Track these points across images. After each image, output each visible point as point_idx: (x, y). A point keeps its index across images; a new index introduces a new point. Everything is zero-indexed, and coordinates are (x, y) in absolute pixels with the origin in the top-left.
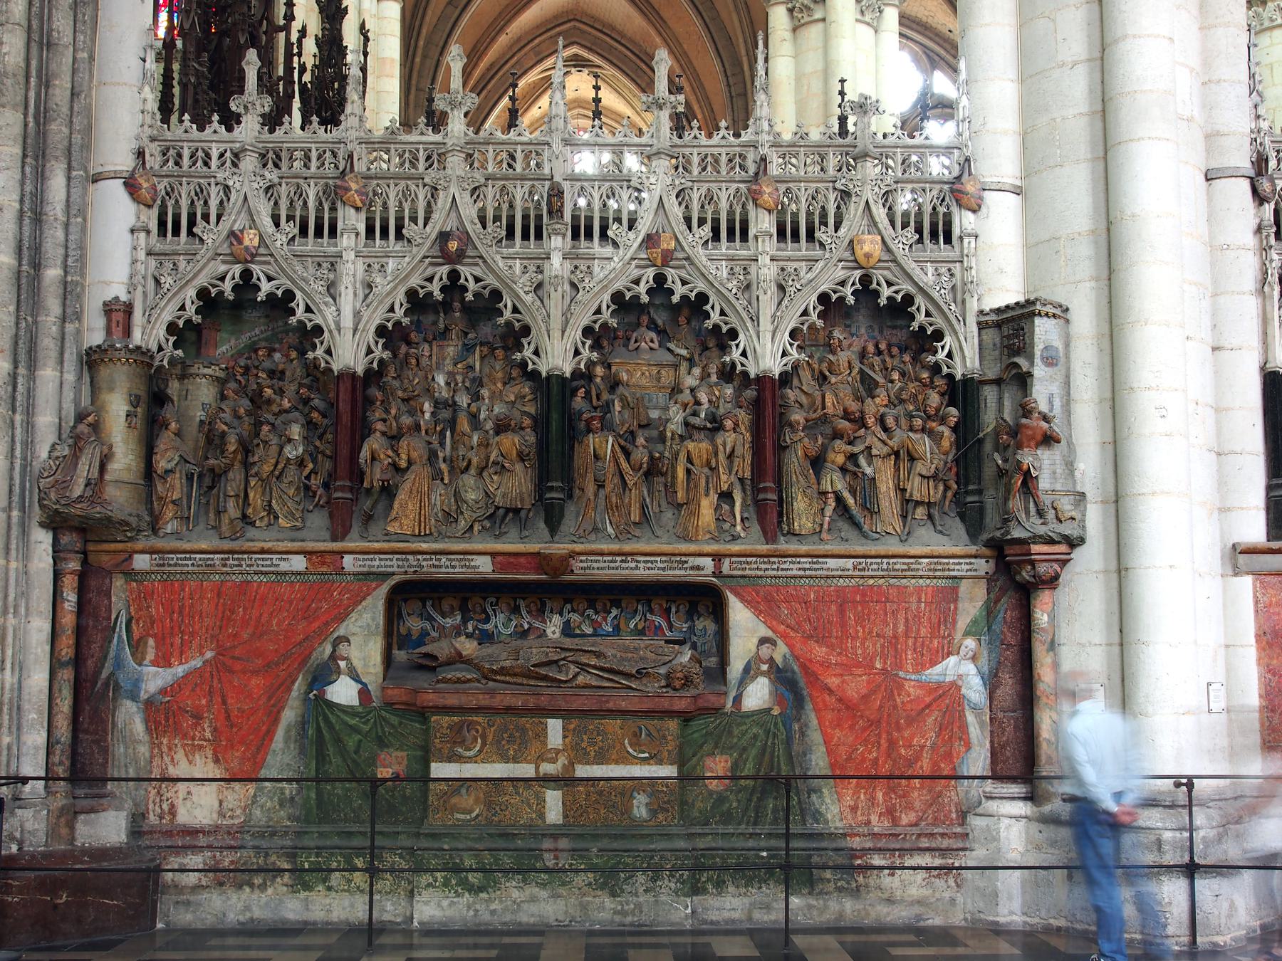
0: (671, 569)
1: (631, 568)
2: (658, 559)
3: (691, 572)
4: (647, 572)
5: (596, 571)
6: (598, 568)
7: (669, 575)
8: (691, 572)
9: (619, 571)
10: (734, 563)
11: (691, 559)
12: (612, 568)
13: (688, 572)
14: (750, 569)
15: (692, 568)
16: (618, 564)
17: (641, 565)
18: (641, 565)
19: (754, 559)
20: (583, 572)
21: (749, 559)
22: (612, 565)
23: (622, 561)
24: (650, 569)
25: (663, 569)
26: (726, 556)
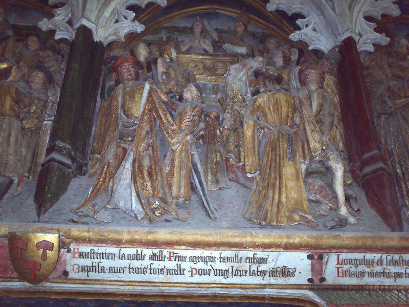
0: (239, 273)
1: (169, 272)
2: (216, 253)
3: (273, 280)
4: (197, 279)
5: (107, 276)
6: (111, 270)
7: (233, 285)
8: (273, 280)
9: (147, 277)
10: (345, 262)
11: (272, 255)
12: (136, 270)
13: (268, 280)
14: (372, 275)
15: (273, 273)
16: (146, 262)
17: (187, 265)
18: (187, 265)
19: (377, 256)
20: (83, 275)
21: (369, 256)
22: (136, 264)
23: (153, 257)
24: (201, 272)
25: (224, 273)
26: (331, 248)
